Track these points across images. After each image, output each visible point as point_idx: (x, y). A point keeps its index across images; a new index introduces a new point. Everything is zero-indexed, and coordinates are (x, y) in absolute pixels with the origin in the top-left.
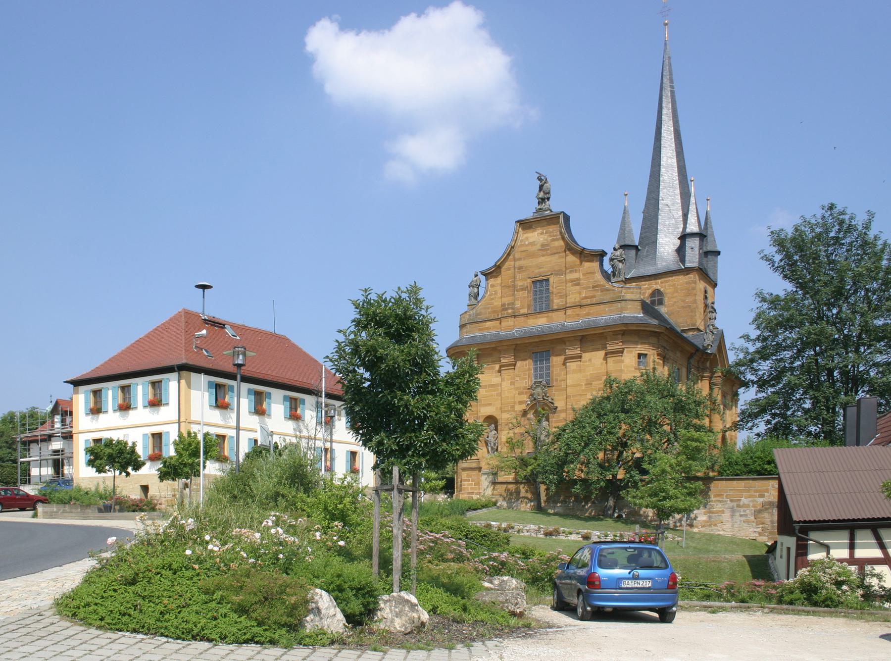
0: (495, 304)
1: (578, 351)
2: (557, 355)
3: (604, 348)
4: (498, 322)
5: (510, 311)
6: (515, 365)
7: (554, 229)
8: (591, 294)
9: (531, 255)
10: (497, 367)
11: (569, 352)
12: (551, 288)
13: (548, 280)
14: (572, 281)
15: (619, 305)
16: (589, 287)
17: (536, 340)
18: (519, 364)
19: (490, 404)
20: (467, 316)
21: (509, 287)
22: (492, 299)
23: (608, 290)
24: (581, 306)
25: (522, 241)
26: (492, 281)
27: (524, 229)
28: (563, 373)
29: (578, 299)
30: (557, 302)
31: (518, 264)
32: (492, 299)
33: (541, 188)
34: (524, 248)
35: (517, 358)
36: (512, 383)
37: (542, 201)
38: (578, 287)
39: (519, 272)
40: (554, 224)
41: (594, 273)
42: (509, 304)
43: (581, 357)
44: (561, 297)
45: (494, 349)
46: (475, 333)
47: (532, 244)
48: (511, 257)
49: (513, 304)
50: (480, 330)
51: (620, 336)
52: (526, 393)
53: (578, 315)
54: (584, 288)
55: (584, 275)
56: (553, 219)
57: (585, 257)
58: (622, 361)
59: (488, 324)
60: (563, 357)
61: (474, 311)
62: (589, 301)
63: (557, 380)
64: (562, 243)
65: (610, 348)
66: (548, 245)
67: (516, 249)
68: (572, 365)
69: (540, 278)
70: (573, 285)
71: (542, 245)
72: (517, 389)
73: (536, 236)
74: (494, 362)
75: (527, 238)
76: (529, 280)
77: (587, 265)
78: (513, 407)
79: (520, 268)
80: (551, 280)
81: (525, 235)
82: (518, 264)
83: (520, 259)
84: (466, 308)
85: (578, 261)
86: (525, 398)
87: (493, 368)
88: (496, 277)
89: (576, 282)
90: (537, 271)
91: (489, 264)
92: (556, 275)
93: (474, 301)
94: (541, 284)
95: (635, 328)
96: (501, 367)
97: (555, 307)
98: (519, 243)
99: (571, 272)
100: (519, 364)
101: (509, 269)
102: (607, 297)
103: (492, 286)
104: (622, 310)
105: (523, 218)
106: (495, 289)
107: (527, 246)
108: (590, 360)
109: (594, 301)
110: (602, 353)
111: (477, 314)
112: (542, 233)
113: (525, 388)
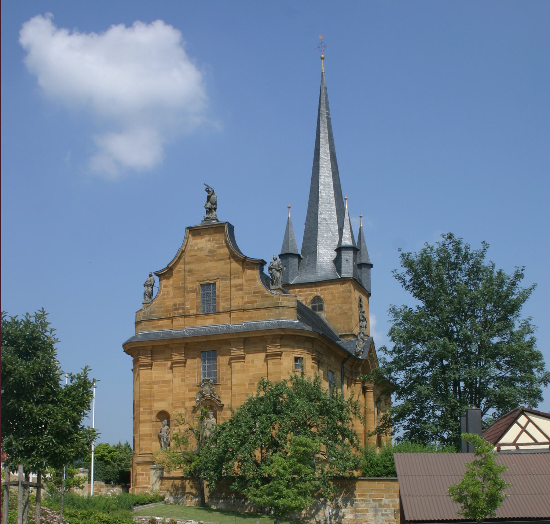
0: (168, 303)
1: (241, 352)
2: (223, 355)
3: (265, 350)
4: (170, 321)
5: (180, 311)
6: (185, 363)
7: (220, 237)
8: (252, 299)
9: (200, 260)
10: (169, 364)
11: (234, 353)
12: (217, 292)
13: (214, 284)
14: (236, 286)
15: (277, 311)
16: (250, 293)
17: (205, 340)
18: (189, 361)
19: (163, 400)
20: (142, 314)
21: (180, 288)
22: (165, 299)
23: (267, 296)
24: (244, 310)
25: (191, 246)
26: (164, 282)
27: (193, 235)
28: (229, 372)
29: (241, 304)
30: (222, 305)
31: (188, 267)
32: (165, 299)
33: (209, 198)
34: (193, 253)
35: (187, 357)
36: (183, 380)
37: (210, 210)
38: (241, 292)
39: (189, 275)
40: (220, 233)
41: (255, 280)
42: (180, 305)
43: (244, 358)
44: (226, 300)
45: (167, 347)
46: (149, 330)
47: (201, 249)
48: (182, 261)
49: (183, 304)
50: (154, 327)
51: (278, 340)
52: (196, 390)
53: (241, 318)
54: (247, 293)
55: (246, 281)
56: (219, 228)
57: (247, 265)
58: (281, 364)
59: (161, 322)
60: (228, 358)
61: (149, 309)
62: (250, 306)
63: (223, 379)
64: (226, 250)
65: (270, 350)
66: (214, 251)
67: (187, 254)
68: (237, 365)
69: (208, 282)
70: (236, 290)
71: (210, 252)
72: (187, 386)
73: (204, 243)
74: (167, 359)
75: (196, 244)
76: (198, 283)
77: (249, 272)
78: (184, 403)
79: (190, 271)
80: (218, 284)
81: (195, 241)
82: (188, 267)
83: (189, 263)
84: (141, 306)
85: (241, 268)
86: (194, 394)
87: (165, 365)
88: (168, 278)
89: (239, 288)
90: (205, 275)
91: (162, 265)
92: (222, 279)
93: (148, 300)
94: (208, 288)
95: (291, 333)
96: (172, 364)
97: (221, 310)
98: (189, 248)
99: (235, 278)
100: (189, 361)
101: (180, 272)
102: (267, 303)
103: (165, 286)
104: (279, 316)
105: (193, 225)
106: (167, 289)
107: (196, 251)
108: (253, 361)
109: (255, 305)
110: (263, 355)
111: (151, 313)
112: (209, 240)
113: (194, 385)
